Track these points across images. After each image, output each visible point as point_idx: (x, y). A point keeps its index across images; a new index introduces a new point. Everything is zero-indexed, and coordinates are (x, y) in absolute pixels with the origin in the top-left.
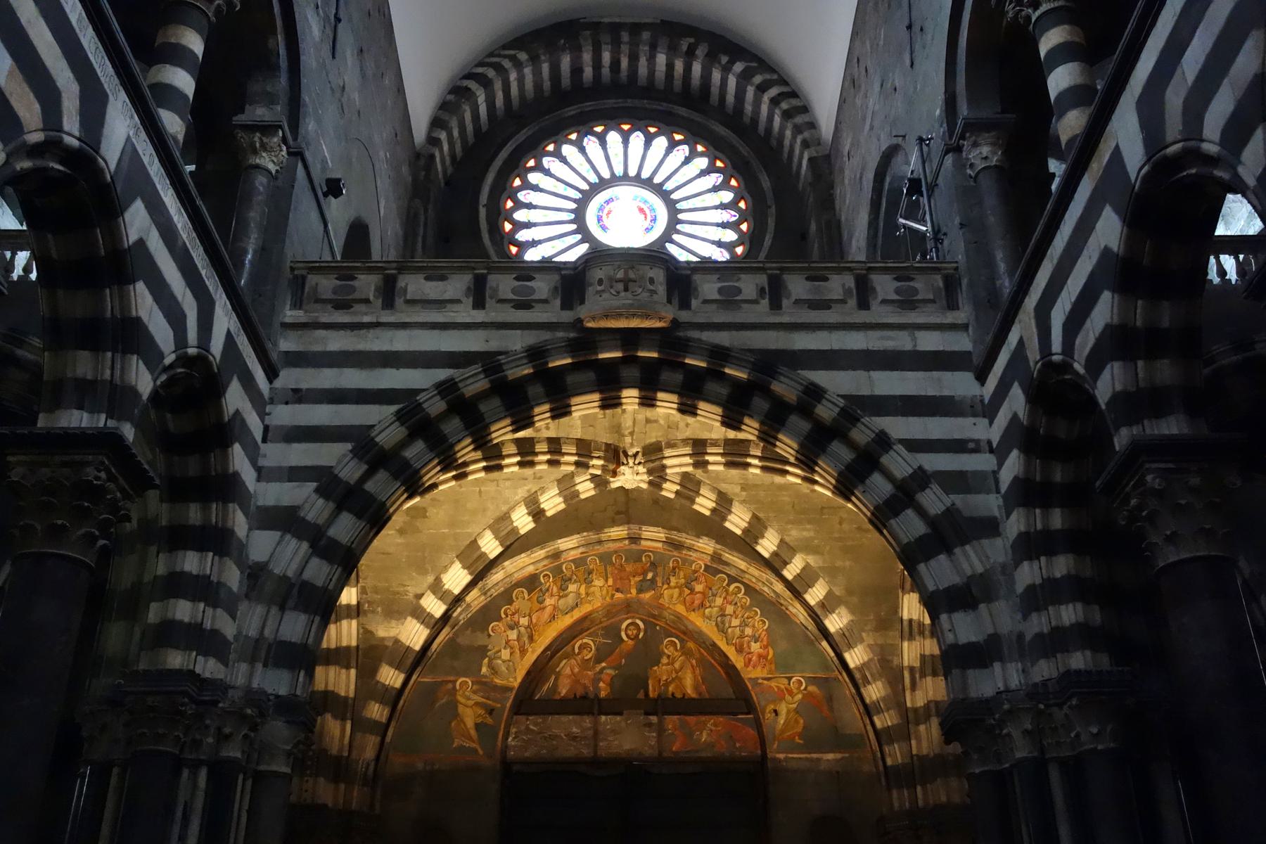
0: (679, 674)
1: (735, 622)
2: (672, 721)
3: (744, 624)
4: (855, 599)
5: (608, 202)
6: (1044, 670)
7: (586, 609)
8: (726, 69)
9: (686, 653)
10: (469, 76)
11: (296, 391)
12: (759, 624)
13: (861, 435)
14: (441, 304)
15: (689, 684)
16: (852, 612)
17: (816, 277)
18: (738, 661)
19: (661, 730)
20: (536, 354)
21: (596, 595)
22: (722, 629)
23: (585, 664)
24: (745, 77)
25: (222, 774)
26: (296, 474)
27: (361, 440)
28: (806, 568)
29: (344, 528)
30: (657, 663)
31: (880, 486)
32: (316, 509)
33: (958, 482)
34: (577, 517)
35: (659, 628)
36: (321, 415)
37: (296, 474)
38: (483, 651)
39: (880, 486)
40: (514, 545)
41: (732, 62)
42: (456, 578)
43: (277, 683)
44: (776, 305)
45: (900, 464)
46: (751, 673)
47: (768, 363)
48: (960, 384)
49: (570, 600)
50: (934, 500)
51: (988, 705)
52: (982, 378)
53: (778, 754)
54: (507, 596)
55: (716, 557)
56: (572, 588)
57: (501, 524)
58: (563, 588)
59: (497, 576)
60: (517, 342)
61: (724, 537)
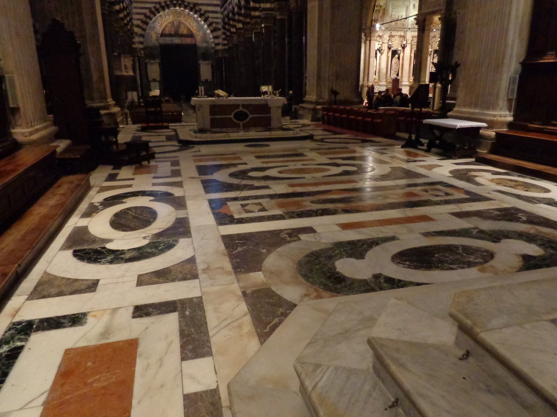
2: (183, 38)
6: (223, 47)
7: (169, 21)
12: (195, 24)
15: (185, 32)
22: (190, 24)
25: (139, 58)
26: (138, 20)
27: (145, 15)
29: (144, 26)
31: (208, 22)
32: (141, 24)
33: (217, 23)
35: (180, 23)
37: (138, 20)
38: (155, 27)
45: (210, 20)
47: (195, 5)
48: (218, 9)
50: (214, 25)
52: (221, 8)
53: (198, 44)
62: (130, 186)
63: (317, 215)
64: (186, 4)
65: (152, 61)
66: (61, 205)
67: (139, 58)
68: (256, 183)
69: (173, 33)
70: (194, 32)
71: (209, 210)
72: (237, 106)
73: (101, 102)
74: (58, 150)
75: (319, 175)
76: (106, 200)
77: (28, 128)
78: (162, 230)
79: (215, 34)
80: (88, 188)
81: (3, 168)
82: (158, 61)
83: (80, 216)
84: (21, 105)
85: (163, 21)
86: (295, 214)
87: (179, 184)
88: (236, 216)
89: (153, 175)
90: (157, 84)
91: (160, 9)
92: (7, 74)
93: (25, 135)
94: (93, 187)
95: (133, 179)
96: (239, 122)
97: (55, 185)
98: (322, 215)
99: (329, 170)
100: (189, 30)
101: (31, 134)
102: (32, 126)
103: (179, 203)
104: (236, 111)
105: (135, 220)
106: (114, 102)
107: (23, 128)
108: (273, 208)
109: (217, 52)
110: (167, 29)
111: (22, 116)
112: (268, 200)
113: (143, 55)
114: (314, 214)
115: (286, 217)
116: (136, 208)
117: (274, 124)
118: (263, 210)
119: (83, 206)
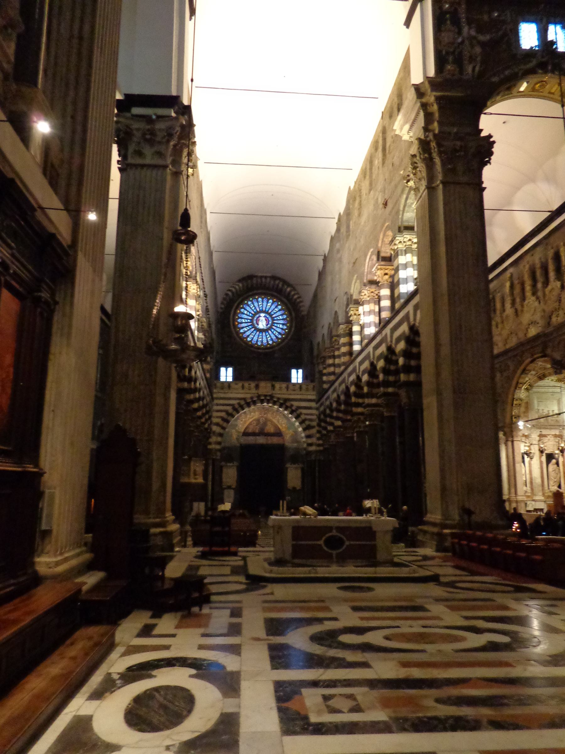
0: (270, 429)
2: (269, 438)
5: (258, 317)
10: (229, 290)
12: (285, 421)
13: (298, 412)
14: (237, 389)
15: (272, 430)
20: (252, 398)
21: (256, 415)
22: (278, 422)
26: (217, 417)
29: (225, 424)
31: (300, 419)
33: (311, 420)
35: (267, 420)
37: (217, 417)
38: (237, 425)
39: (300, 419)
43: (218, 447)
44: (287, 390)
45: (303, 417)
47: (286, 400)
48: (313, 404)
50: (307, 423)
51: (311, 452)
52: (317, 403)
60: (248, 396)
62: (167, 647)
63: (445, 729)
64: (275, 399)
65: (229, 464)
66: (64, 676)
67: (214, 460)
68: (350, 657)
69: (257, 431)
70: (283, 430)
71: (272, 703)
72: (330, 529)
73: (157, 517)
74: (85, 588)
75: (448, 647)
76: (130, 669)
77: (55, 556)
78: (197, 734)
79: (308, 432)
80: (111, 646)
81: (6, 617)
82: (236, 463)
83: (87, 695)
84: (55, 528)
85: (247, 419)
86: (409, 723)
87: (235, 650)
88: (314, 719)
89: (202, 630)
90: (232, 492)
91: (245, 406)
92: (49, 489)
93: (51, 565)
94: (118, 645)
95: (174, 636)
96: (330, 551)
97: (68, 642)
98: (454, 729)
99: (463, 639)
100: (276, 427)
101: (57, 564)
102: (61, 554)
103: (229, 684)
104: (327, 535)
105: (161, 711)
106: (174, 517)
107: (49, 557)
108: (372, 707)
109: (309, 453)
111: (53, 540)
112: (365, 689)
113: (218, 458)
114: (441, 726)
115: (394, 728)
116: (167, 688)
117: (381, 556)
118: (357, 709)
119: (96, 679)
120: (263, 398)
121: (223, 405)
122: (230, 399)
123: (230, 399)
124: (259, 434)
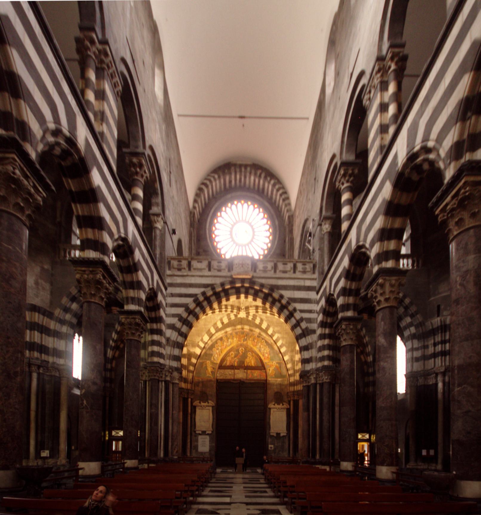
1: (263, 349)
2: (249, 371)
3: (264, 350)
4: (287, 345)
8: (269, 183)
9: (252, 356)
11: (172, 294)
12: (268, 350)
16: (286, 347)
17: (285, 264)
18: (263, 358)
19: (247, 373)
21: (234, 342)
22: (260, 351)
23: (232, 358)
24: (274, 185)
28: (278, 337)
30: (246, 358)
34: (231, 324)
35: (247, 350)
36: (177, 300)
40: (218, 330)
41: (271, 180)
42: (206, 338)
46: (265, 361)
49: (229, 343)
54: (216, 342)
55: (260, 334)
56: (230, 340)
57: (215, 325)
58: (228, 340)
59: (214, 337)
61: (261, 329)
110: (229, 359)
120: (238, 285)
121: (181, 295)
122: (191, 285)
123: (191, 285)
124: (238, 368)
